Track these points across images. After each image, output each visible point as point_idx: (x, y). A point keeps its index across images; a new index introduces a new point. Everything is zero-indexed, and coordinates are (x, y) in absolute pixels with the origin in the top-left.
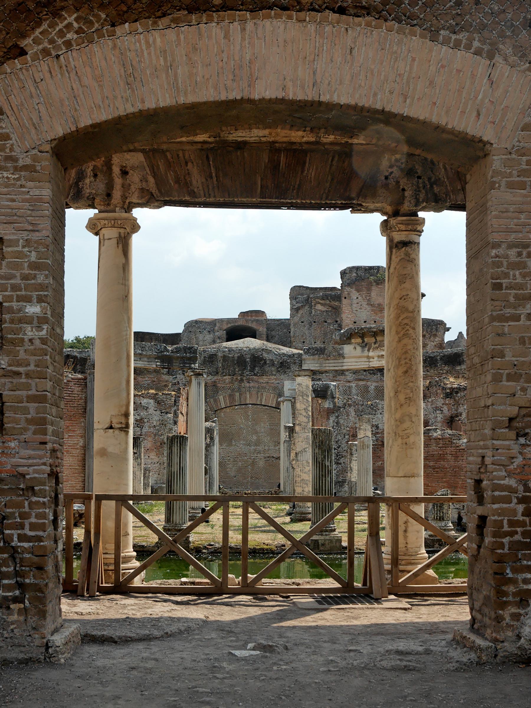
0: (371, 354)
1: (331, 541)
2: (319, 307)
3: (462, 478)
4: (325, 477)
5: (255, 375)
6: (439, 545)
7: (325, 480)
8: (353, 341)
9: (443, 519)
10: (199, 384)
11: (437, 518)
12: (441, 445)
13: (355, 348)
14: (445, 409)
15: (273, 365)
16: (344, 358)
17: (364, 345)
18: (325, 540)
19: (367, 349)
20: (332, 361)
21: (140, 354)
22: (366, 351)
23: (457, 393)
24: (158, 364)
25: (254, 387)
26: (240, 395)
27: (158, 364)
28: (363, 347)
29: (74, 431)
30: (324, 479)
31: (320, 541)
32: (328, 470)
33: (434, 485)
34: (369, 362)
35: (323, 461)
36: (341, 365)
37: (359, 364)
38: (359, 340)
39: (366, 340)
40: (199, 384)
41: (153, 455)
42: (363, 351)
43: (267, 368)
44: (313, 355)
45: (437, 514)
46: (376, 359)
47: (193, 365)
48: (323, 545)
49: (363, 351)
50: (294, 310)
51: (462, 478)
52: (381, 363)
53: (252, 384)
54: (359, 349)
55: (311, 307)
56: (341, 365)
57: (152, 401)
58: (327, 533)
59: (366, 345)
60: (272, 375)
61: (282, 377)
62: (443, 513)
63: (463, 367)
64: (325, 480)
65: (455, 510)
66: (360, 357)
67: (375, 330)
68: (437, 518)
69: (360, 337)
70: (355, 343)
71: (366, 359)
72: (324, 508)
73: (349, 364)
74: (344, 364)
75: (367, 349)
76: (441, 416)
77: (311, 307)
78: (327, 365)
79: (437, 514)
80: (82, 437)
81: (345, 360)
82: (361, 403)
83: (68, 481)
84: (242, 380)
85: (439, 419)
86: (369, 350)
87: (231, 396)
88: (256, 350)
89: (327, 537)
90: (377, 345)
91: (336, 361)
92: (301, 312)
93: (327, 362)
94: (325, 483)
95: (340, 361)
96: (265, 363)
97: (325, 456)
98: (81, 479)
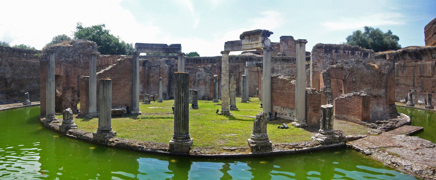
0: (253, 43)
8: (245, 38)
41: (203, 86)
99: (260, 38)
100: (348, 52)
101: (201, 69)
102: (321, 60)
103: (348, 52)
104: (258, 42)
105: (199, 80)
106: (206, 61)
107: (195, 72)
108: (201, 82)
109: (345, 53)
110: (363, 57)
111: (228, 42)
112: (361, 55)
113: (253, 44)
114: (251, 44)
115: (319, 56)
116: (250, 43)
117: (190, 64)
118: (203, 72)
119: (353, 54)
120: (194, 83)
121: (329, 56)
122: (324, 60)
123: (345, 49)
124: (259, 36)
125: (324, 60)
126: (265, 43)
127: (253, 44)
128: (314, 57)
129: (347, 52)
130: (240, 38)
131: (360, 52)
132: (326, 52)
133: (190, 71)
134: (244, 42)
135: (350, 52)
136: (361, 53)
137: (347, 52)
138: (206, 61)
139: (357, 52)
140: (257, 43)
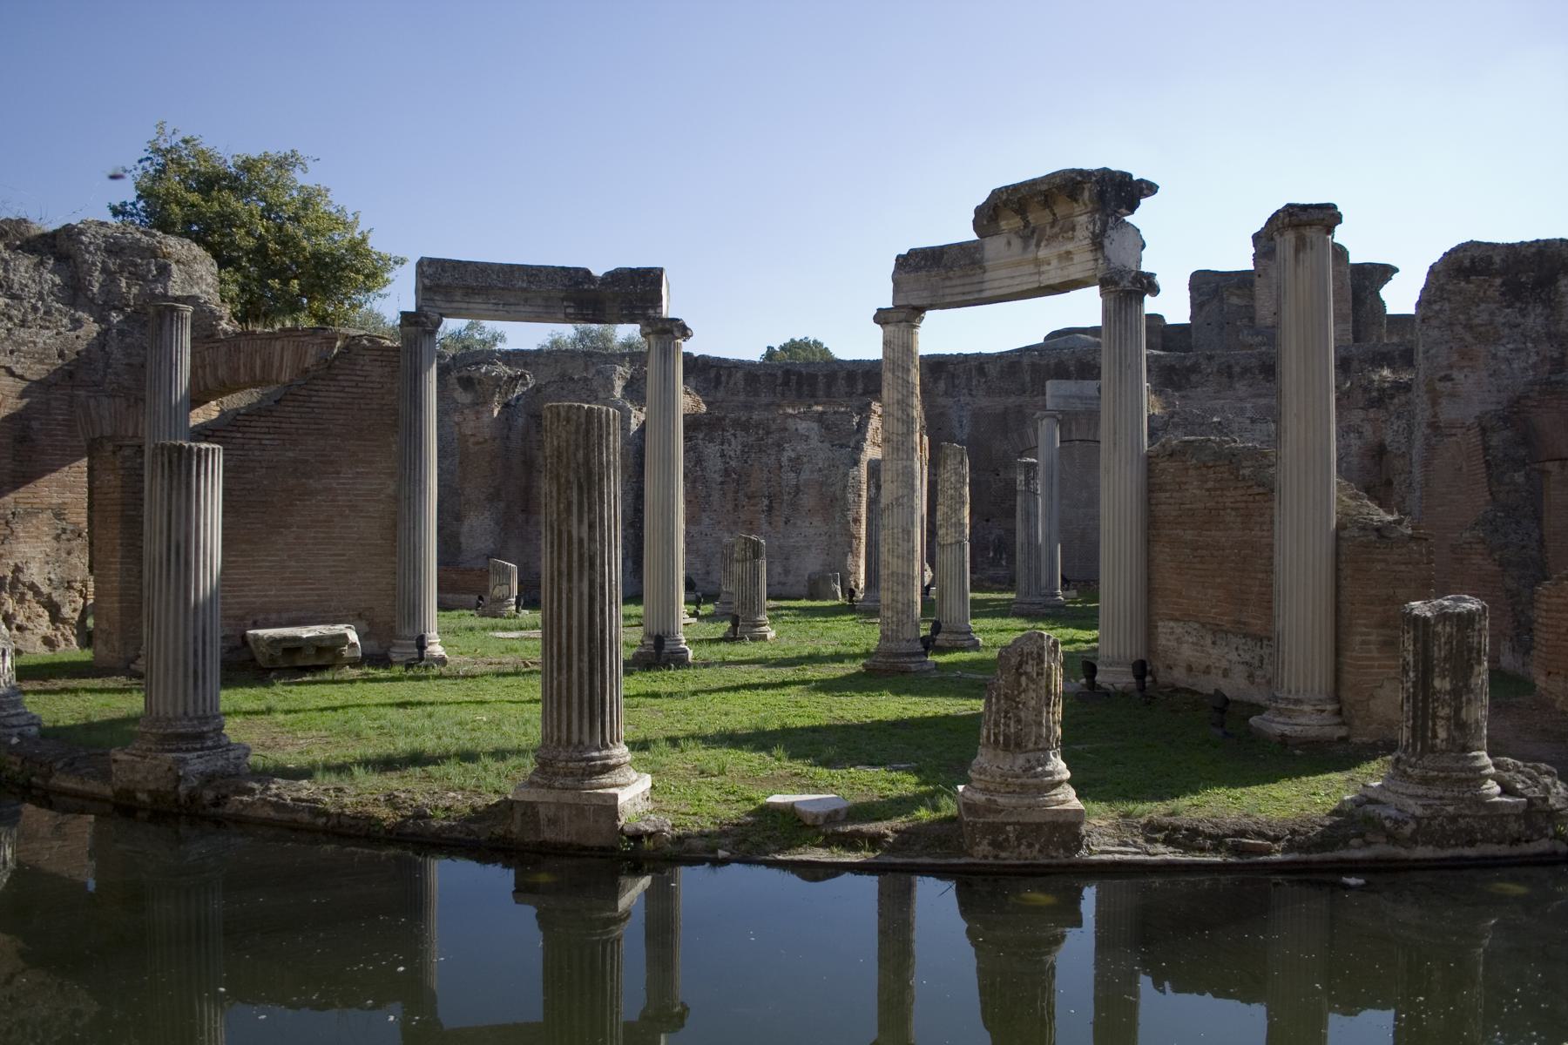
0: (1043, 253)
1: (579, 810)
2: (1235, 300)
3: (1260, 576)
4: (570, 580)
6: (993, 844)
7: (570, 590)
8: (1003, 224)
9: (1018, 745)
11: (996, 741)
12: (1210, 484)
13: (1009, 243)
14: (1368, 429)
17: (1029, 235)
18: (560, 806)
19: (1034, 242)
20: (958, 282)
21: (524, 290)
22: (1033, 247)
23: (1392, 397)
24: (570, 310)
27: (570, 310)
28: (1026, 240)
30: (564, 585)
31: (541, 809)
32: (581, 556)
34: (1040, 273)
36: (977, 287)
37: (1017, 281)
38: (1016, 222)
39: (1031, 218)
41: (817, 521)
42: (1025, 248)
44: (917, 269)
45: (997, 724)
46: (1054, 263)
47: (651, 312)
48: (553, 822)
49: (1025, 248)
50: (1196, 306)
51: (1260, 576)
52: (1065, 272)
54: (1017, 243)
55: (1221, 300)
56: (977, 287)
57: (815, 425)
58: (569, 781)
59: (1033, 232)
62: (1019, 721)
64: (570, 590)
65: (1241, 667)
66: (1019, 264)
67: (1044, 187)
68: (996, 741)
69: (1017, 212)
70: (1010, 231)
71: (1032, 268)
72: (564, 692)
73: (996, 284)
74: (986, 286)
75: (1034, 242)
76: (1358, 442)
78: (947, 291)
79: (997, 724)
81: (987, 276)
82: (1200, 420)
85: (1354, 449)
86: (1038, 245)
89: (568, 797)
90: (1056, 229)
91: (967, 280)
92: (1207, 308)
93: (948, 283)
94: (570, 600)
95: (976, 279)
97: (570, 504)
101: (802, 426)
105: (798, 490)
106: (841, 384)
107: (779, 446)
108: (808, 500)
111: (913, 253)
115: (1469, 327)
117: (764, 399)
118: (814, 442)
120: (770, 508)
121: (1534, 320)
122: (1501, 351)
124: (1078, 208)
125: (1501, 351)
126: (1110, 248)
130: (977, 225)
132: (1514, 293)
133: (751, 440)
134: (995, 247)
138: (841, 384)
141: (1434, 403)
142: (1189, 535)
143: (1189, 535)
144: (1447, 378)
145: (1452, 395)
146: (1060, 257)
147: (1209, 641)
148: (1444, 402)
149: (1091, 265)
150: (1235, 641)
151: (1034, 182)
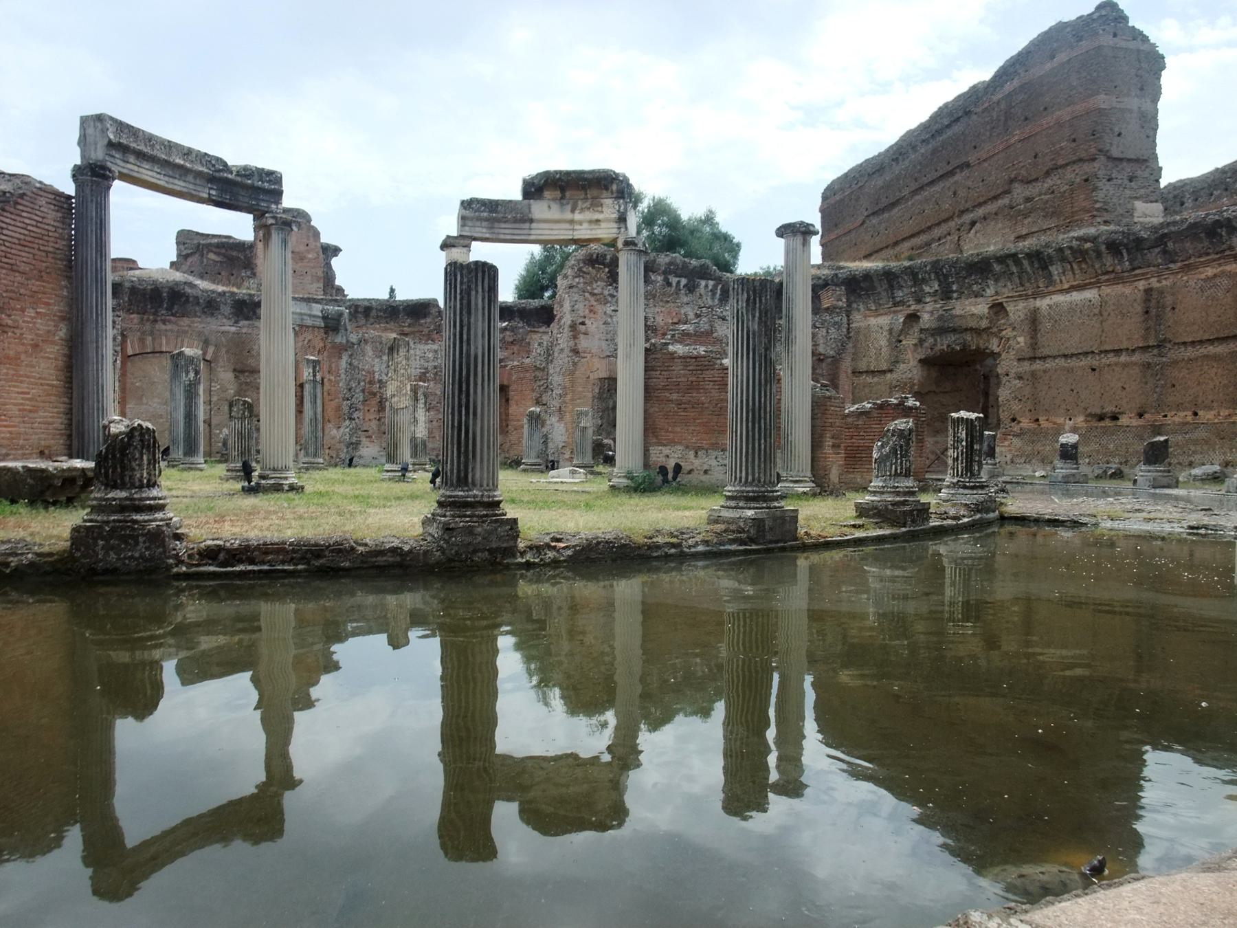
0: (578, 216)
2: (212, 256)
5: (173, 315)
8: (547, 194)
10: (285, 242)
15: (198, 303)
16: (531, 221)
24: (213, 192)
25: (172, 331)
26: (154, 339)
27: (213, 192)
29: (48, 304)
33: (678, 429)
35: (767, 349)
38: (558, 194)
40: (285, 242)
43: (189, 307)
46: (585, 225)
47: (273, 206)
53: (169, 327)
55: (202, 255)
60: (196, 316)
61: (209, 319)
63: (429, 320)
67: (590, 176)
71: (567, 226)
75: (569, 207)
77: (202, 255)
80: (63, 319)
81: (534, 225)
83: (36, 411)
84: (156, 321)
86: (573, 211)
87: (142, 341)
88: (177, 283)
92: (190, 260)
96: (187, 301)
98: (62, 408)
99: (609, 202)
100: (679, 282)
102: (600, 309)
103: (679, 282)
104: (600, 216)
109: (669, 284)
110: (721, 300)
112: (713, 292)
113: (580, 223)
114: (572, 222)
115: (593, 294)
116: (569, 216)
119: (691, 288)
123: (670, 273)
124: (605, 194)
127: (580, 223)
128: (576, 297)
129: (674, 280)
131: (711, 283)
134: (540, 209)
135: (684, 281)
136: (715, 287)
137: (674, 280)
139: (703, 283)
140: (598, 221)
141: (575, 337)
142: (674, 396)
143: (674, 396)
144: (583, 324)
145: (586, 334)
146: (590, 222)
147: (692, 453)
148: (582, 336)
149: (615, 231)
150: (715, 453)
151: (583, 172)
